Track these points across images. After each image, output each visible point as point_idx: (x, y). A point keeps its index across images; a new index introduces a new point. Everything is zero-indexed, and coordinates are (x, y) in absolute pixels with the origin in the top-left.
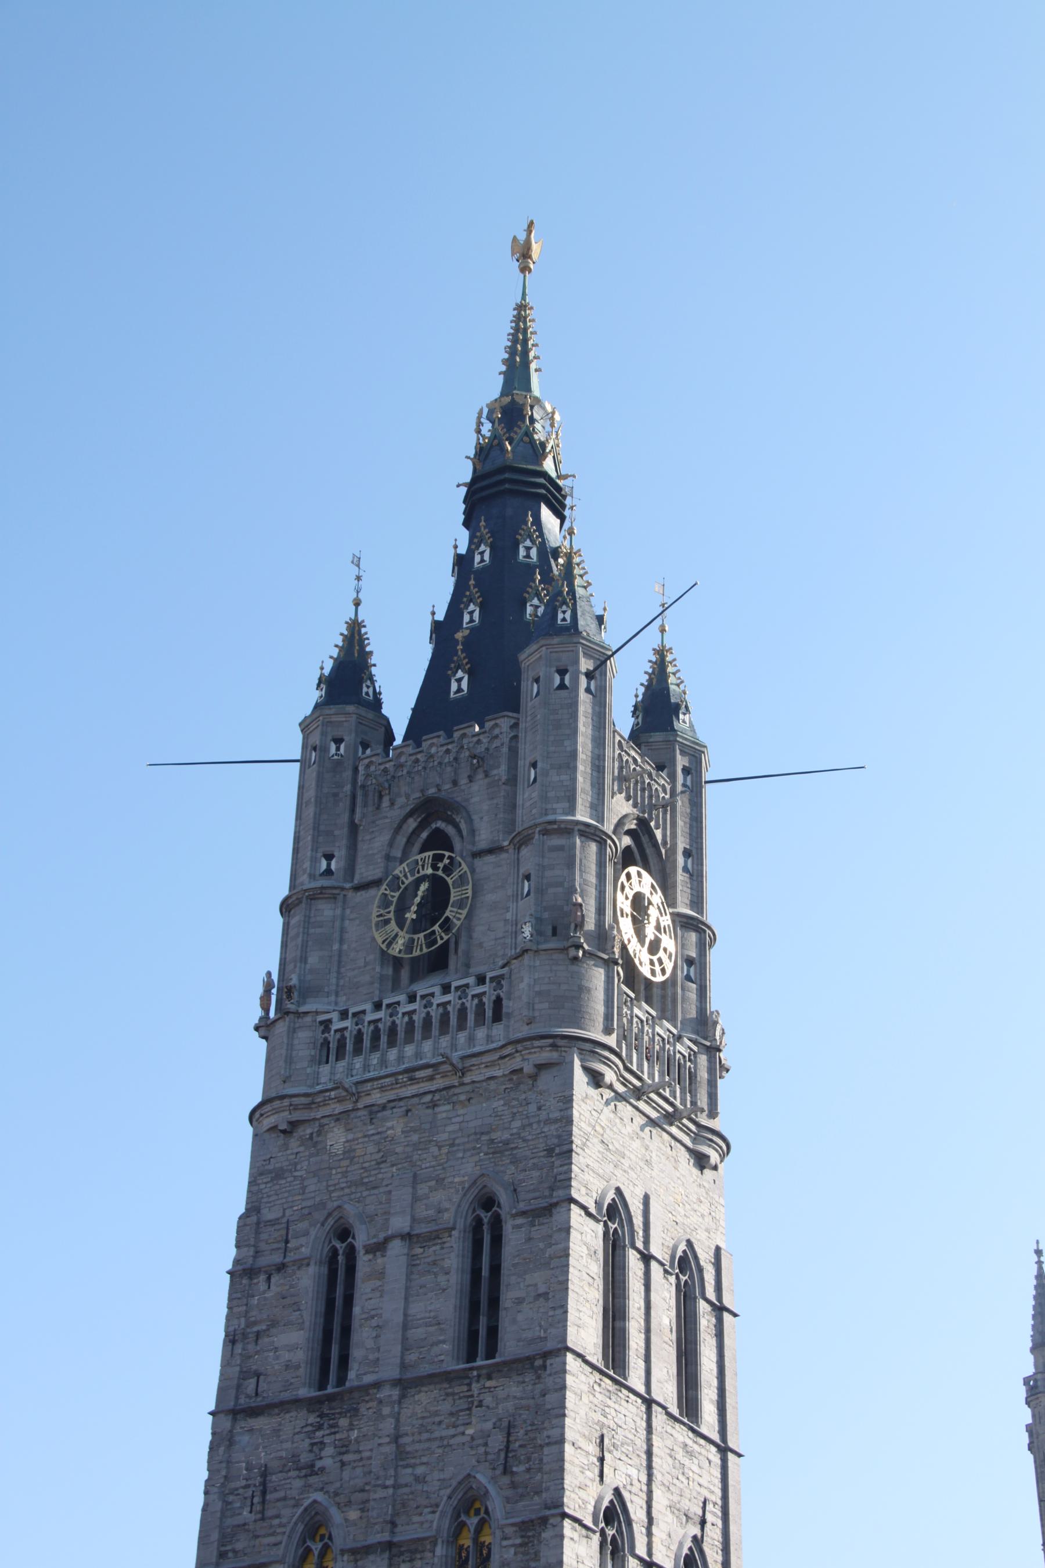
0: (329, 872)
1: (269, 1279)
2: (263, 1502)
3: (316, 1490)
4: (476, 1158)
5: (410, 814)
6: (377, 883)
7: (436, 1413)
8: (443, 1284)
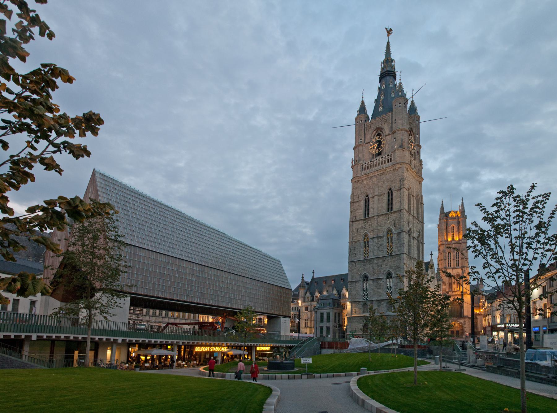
0: (361, 142)
6: (369, 142)
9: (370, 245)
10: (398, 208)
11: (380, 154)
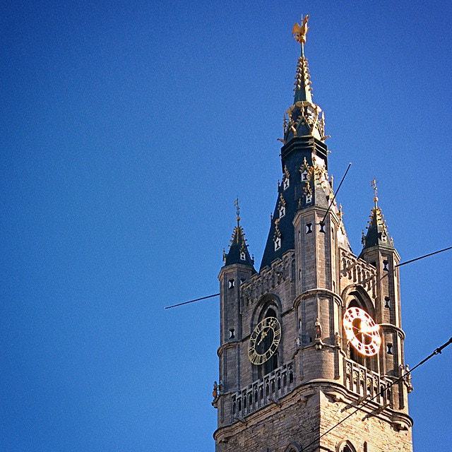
0: (233, 336)
11: (271, 365)
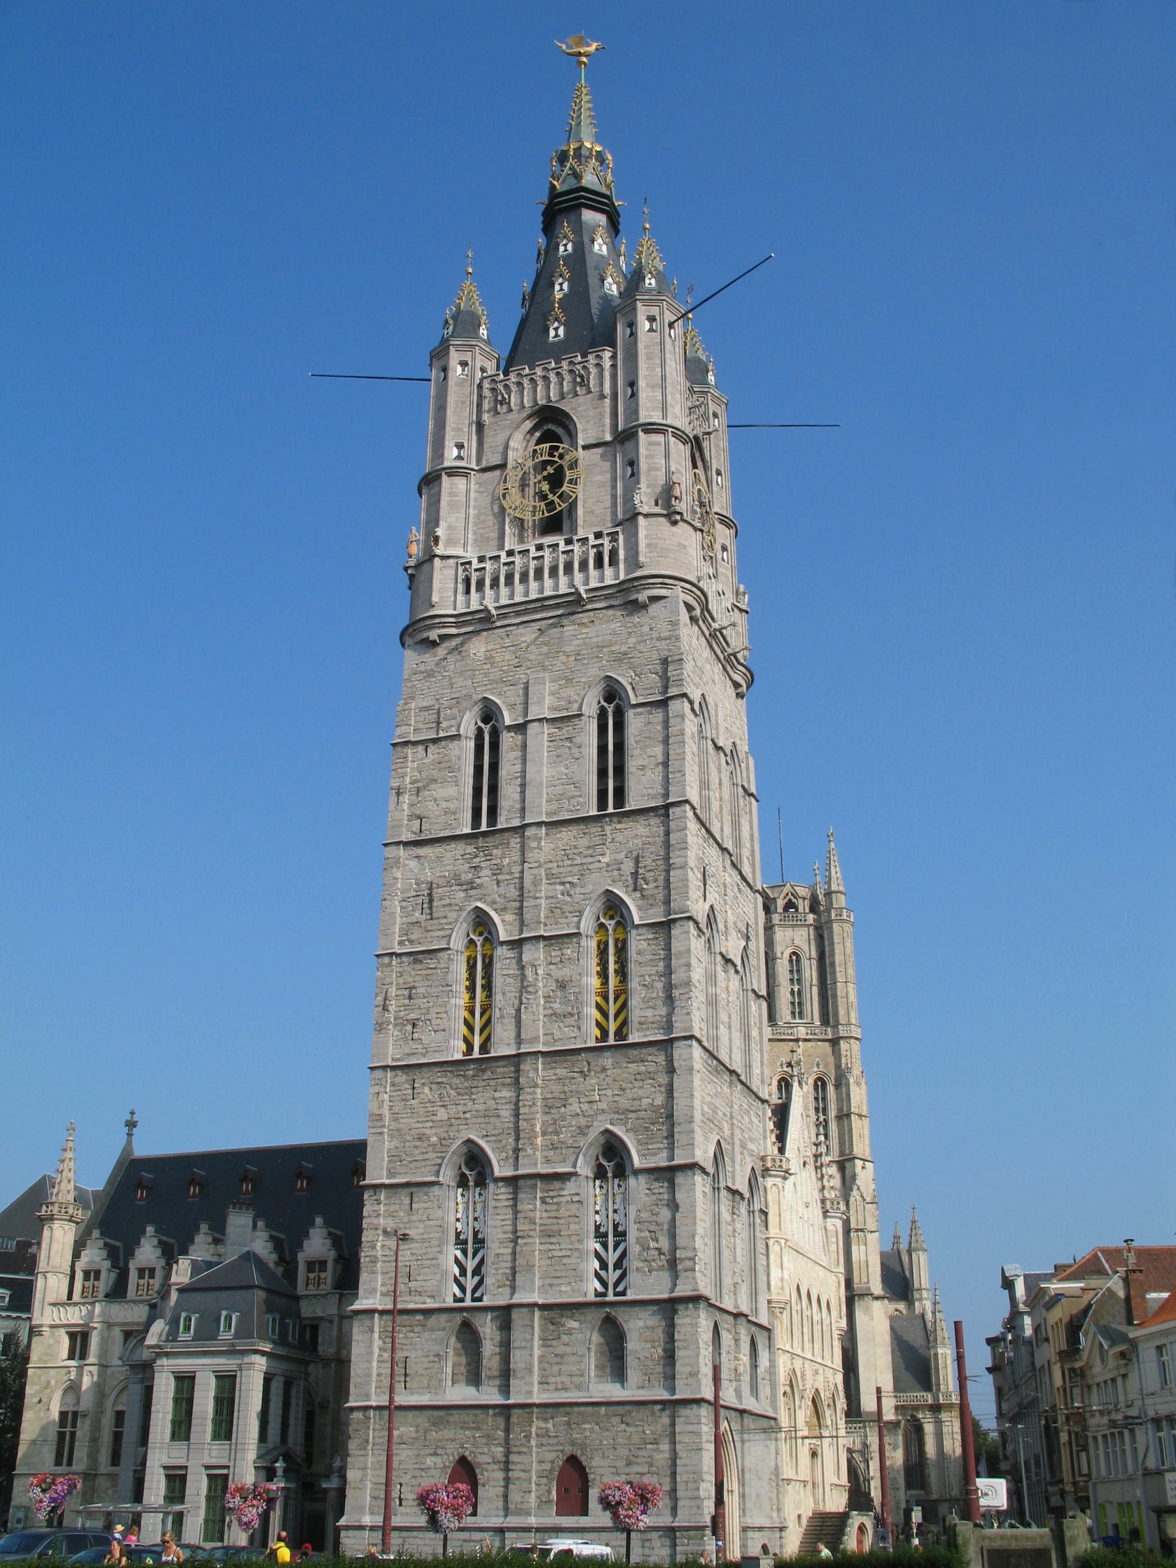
0: (459, 458)
1: (427, 747)
2: (431, 908)
3: (476, 900)
4: (599, 664)
5: (529, 417)
7: (576, 847)
8: (577, 755)
9: (498, 981)
10: (654, 797)
